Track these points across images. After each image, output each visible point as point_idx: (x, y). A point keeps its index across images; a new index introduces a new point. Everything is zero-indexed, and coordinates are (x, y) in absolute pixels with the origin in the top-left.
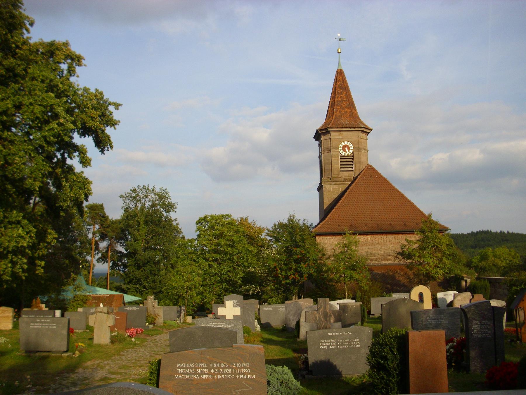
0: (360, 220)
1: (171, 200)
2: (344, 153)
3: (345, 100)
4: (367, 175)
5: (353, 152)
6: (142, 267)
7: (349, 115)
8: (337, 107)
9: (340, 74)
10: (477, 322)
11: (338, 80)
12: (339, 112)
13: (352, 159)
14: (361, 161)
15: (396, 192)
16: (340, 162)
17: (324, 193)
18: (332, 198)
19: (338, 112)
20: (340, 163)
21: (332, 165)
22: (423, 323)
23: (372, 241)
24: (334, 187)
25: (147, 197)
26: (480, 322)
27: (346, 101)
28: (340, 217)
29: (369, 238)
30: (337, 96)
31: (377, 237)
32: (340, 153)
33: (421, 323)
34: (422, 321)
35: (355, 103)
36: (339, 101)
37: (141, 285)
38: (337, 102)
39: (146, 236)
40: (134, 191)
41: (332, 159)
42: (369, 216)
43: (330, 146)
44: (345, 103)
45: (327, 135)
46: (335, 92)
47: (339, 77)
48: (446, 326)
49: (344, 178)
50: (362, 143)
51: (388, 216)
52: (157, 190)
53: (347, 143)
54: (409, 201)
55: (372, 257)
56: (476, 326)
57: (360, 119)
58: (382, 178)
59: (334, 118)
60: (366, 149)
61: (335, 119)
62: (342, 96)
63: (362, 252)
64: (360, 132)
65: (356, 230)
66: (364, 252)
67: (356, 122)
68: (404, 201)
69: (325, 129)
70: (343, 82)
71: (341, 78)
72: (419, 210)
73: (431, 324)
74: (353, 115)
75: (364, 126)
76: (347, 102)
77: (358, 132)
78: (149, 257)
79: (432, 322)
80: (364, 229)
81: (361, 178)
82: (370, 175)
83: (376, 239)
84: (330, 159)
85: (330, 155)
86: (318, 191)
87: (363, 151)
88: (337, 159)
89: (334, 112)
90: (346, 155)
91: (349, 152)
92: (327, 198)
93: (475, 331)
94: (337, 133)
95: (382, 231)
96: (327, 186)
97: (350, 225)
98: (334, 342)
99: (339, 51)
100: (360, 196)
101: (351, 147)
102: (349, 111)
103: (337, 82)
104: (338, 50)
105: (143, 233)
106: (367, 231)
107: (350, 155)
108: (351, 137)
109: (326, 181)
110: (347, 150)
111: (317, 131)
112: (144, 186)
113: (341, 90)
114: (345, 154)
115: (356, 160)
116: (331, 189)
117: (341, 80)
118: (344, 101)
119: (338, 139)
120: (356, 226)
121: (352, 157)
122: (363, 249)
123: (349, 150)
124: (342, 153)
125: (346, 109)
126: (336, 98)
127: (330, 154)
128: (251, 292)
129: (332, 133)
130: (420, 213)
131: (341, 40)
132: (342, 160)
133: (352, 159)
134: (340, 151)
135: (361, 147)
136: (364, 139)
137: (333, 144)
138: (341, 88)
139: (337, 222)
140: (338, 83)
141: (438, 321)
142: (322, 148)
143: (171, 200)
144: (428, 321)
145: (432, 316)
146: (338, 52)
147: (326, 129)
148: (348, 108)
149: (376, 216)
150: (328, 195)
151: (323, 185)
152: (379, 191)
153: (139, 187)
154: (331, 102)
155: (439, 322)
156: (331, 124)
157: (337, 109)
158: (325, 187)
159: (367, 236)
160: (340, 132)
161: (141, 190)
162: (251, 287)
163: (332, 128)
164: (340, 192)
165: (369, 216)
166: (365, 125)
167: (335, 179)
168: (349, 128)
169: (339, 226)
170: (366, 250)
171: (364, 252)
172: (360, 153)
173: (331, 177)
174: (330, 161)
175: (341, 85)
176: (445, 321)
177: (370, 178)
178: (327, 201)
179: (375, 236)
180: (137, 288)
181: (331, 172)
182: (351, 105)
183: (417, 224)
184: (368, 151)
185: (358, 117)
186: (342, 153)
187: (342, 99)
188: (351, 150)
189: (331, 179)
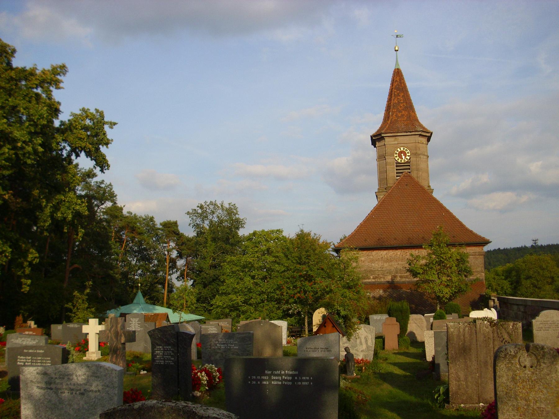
0: (389, 233)
1: (239, 216)
2: (400, 159)
3: (402, 101)
4: (403, 183)
5: (410, 158)
6: (208, 285)
7: (406, 118)
8: (393, 110)
9: (398, 74)
10: (160, 347)
11: (395, 81)
12: (396, 116)
13: (409, 165)
14: (419, 168)
15: (434, 201)
16: (396, 170)
19: (394, 116)
20: (396, 171)
21: (387, 174)
22: (211, 347)
23: (402, 256)
25: (213, 213)
26: (163, 348)
27: (403, 103)
28: (368, 230)
29: (399, 253)
30: (393, 98)
31: (408, 251)
32: (396, 160)
33: (209, 347)
34: (210, 345)
35: (414, 104)
36: (395, 103)
37: (208, 304)
38: (393, 104)
39: (214, 253)
40: (201, 207)
42: (400, 229)
43: (385, 152)
44: (402, 106)
45: (382, 141)
46: (392, 94)
47: (396, 78)
48: (236, 352)
50: (421, 148)
51: (422, 228)
52: (226, 206)
53: (404, 149)
54: (447, 211)
55: (402, 273)
56: (159, 352)
57: (419, 122)
58: (419, 186)
59: (389, 121)
60: (426, 154)
61: (391, 123)
62: (399, 98)
63: (391, 268)
64: (418, 136)
65: (383, 244)
66: (393, 268)
67: (413, 126)
68: (442, 211)
69: (379, 134)
70: (401, 83)
71: (398, 79)
72: (458, 220)
73: (220, 349)
74: (411, 117)
75: (421, 130)
76: (404, 104)
77: (415, 136)
78: (214, 275)
79: (220, 347)
80: (394, 243)
81: (396, 188)
82: (405, 183)
83: (407, 254)
85: (385, 163)
87: (422, 157)
89: (389, 115)
90: (403, 162)
91: (404, 159)
93: (158, 356)
94: (393, 139)
95: (412, 245)
97: (378, 239)
98: (29, 359)
99: (397, 49)
100: (392, 207)
101: (408, 153)
102: (406, 113)
103: (394, 83)
104: (395, 48)
105: (210, 250)
106: (395, 246)
107: (407, 162)
109: (380, 191)
110: (403, 157)
112: (211, 202)
113: (398, 92)
114: (401, 161)
115: (414, 167)
117: (398, 80)
119: (393, 145)
120: (384, 240)
121: (409, 164)
122: (391, 265)
124: (398, 159)
125: (403, 112)
126: (392, 101)
127: (385, 161)
128: (290, 312)
129: (386, 139)
130: (458, 224)
131: (399, 36)
132: (398, 168)
133: (409, 165)
134: (396, 158)
135: (419, 152)
136: (423, 143)
137: (388, 150)
138: (398, 89)
139: (364, 236)
140: (395, 84)
141: (228, 346)
143: (239, 216)
144: (216, 346)
145: (221, 340)
146: (396, 50)
147: (380, 134)
148: (406, 110)
149: (409, 229)
152: (414, 200)
153: (205, 202)
155: (229, 347)
156: (385, 129)
157: (393, 112)
159: (397, 251)
160: (394, 137)
161: (208, 206)
162: (293, 306)
163: (386, 133)
165: (400, 229)
166: (424, 128)
168: (405, 132)
169: (366, 240)
170: (395, 267)
171: (393, 268)
172: (417, 159)
174: (385, 169)
175: (399, 85)
176: (235, 346)
177: (406, 187)
179: (405, 250)
180: (205, 307)
181: (386, 181)
182: (410, 107)
183: (453, 237)
184: (428, 157)
185: (417, 120)
186: (398, 159)
187: (399, 102)
188: (408, 156)
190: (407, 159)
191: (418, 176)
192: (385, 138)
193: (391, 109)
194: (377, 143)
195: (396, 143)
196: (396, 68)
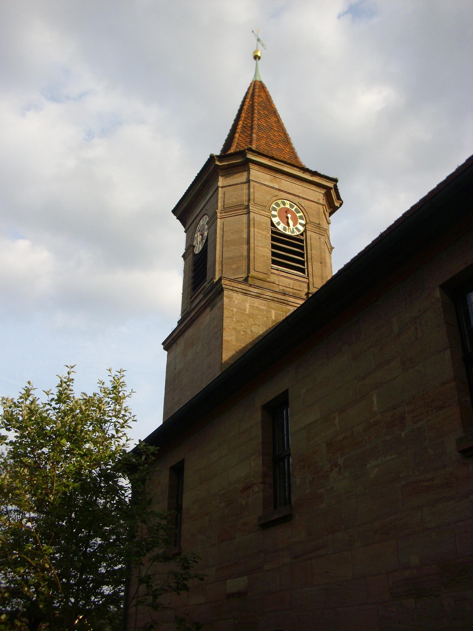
5: (305, 231)
11: (256, 94)
17: (226, 313)
18: (249, 332)
21: (252, 245)
24: (256, 305)
41: (252, 229)
43: (245, 198)
45: (238, 175)
49: (281, 288)
64: (323, 191)
84: (246, 231)
86: (165, 349)
88: (264, 233)
90: (288, 233)
92: (234, 329)
96: (235, 295)
99: (259, 54)
103: (256, 97)
104: (256, 51)
108: (300, 195)
111: (212, 158)
114: (285, 229)
116: (248, 306)
118: (275, 130)
123: (295, 224)
126: (256, 119)
142: (220, 204)
147: (241, 153)
150: (238, 321)
151: (222, 290)
154: (240, 126)
158: (230, 298)
164: (273, 321)
167: (258, 283)
173: (244, 276)
174: (245, 236)
178: (234, 338)
181: (245, 263)
184: (332, 248)
186: (278, 223)
189: (246, 280)
190: (297, 229)
191: (324, 276)
192: (251, 166)
193: (255, 131)
194: (221, 179)
195: (276, 186)
196: (258, 79)
